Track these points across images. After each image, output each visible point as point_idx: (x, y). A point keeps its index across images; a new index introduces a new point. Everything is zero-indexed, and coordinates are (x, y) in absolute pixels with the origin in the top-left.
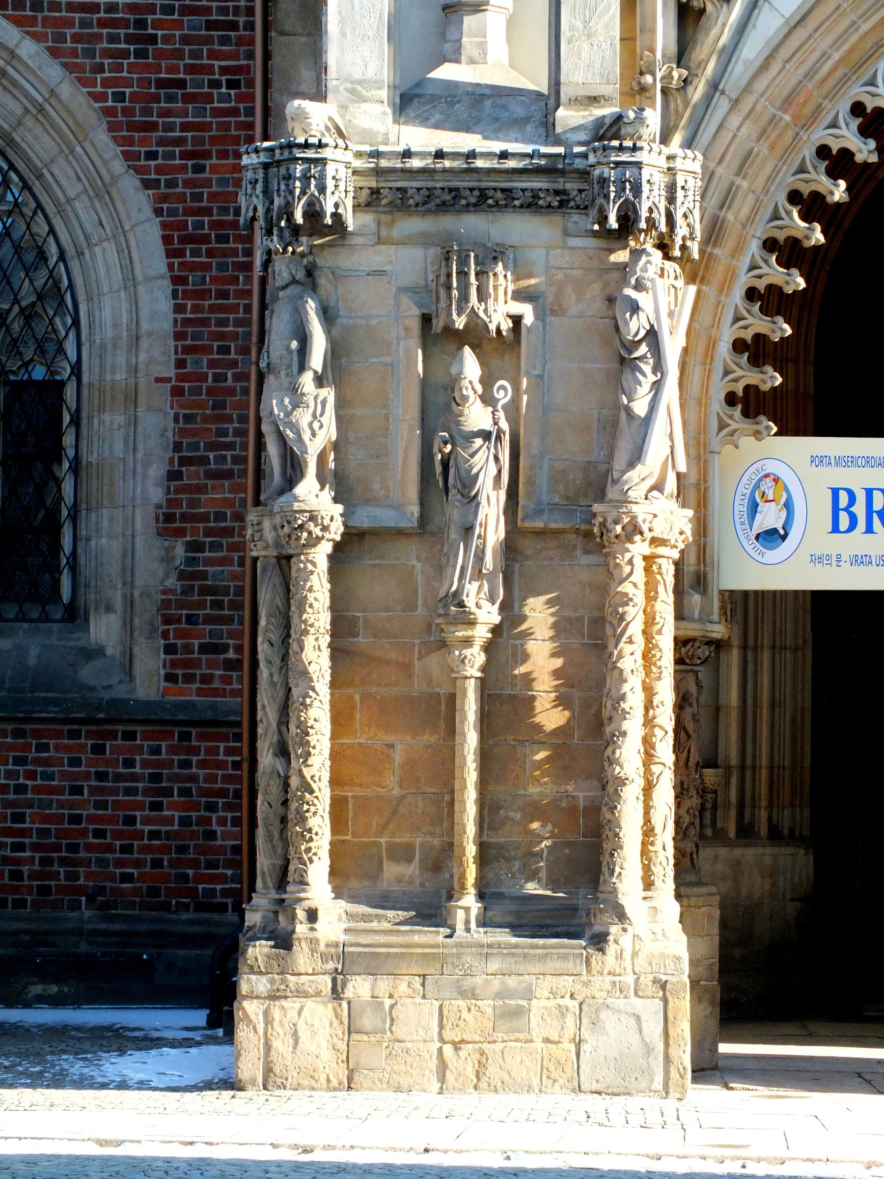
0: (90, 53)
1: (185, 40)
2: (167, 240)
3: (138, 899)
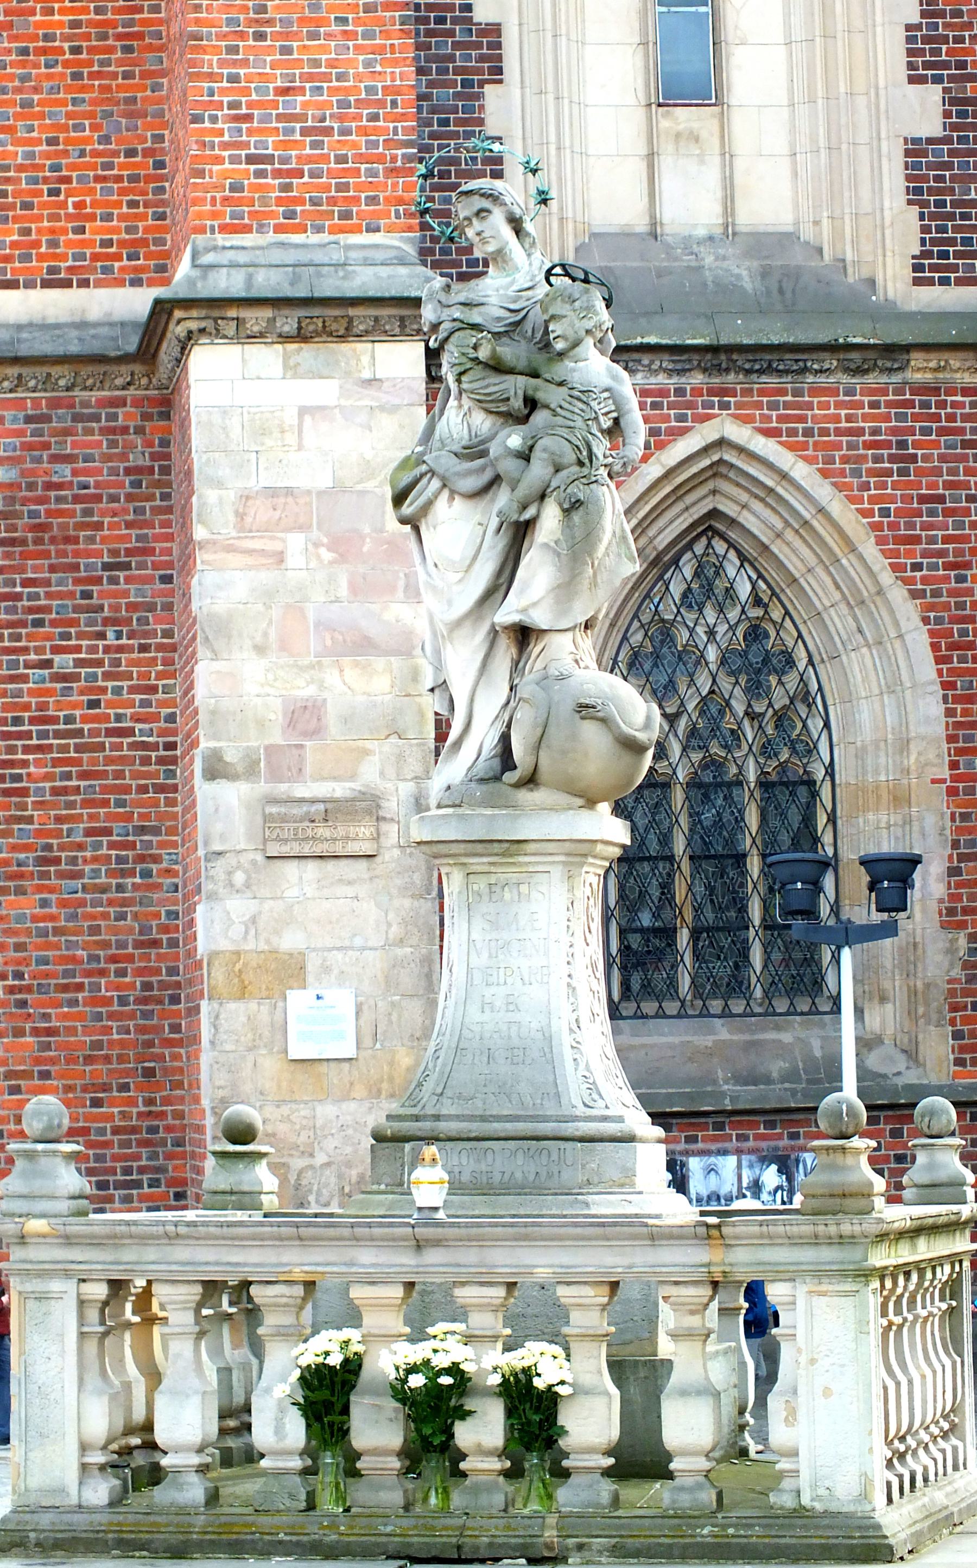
0: (857, 473)
1: (942, 458)
2: (935, 647)
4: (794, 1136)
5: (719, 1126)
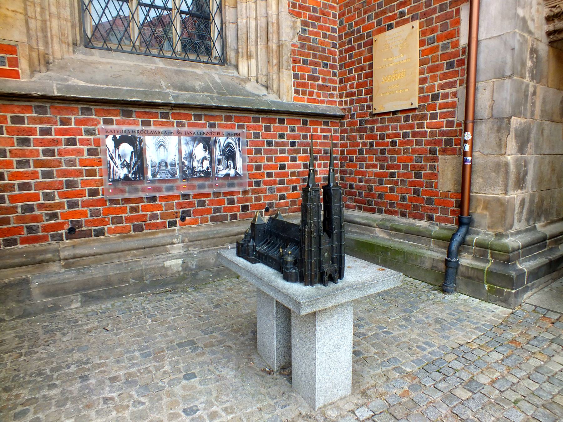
3: (287, 208)
4: (212, 126)
5: (165, 116)
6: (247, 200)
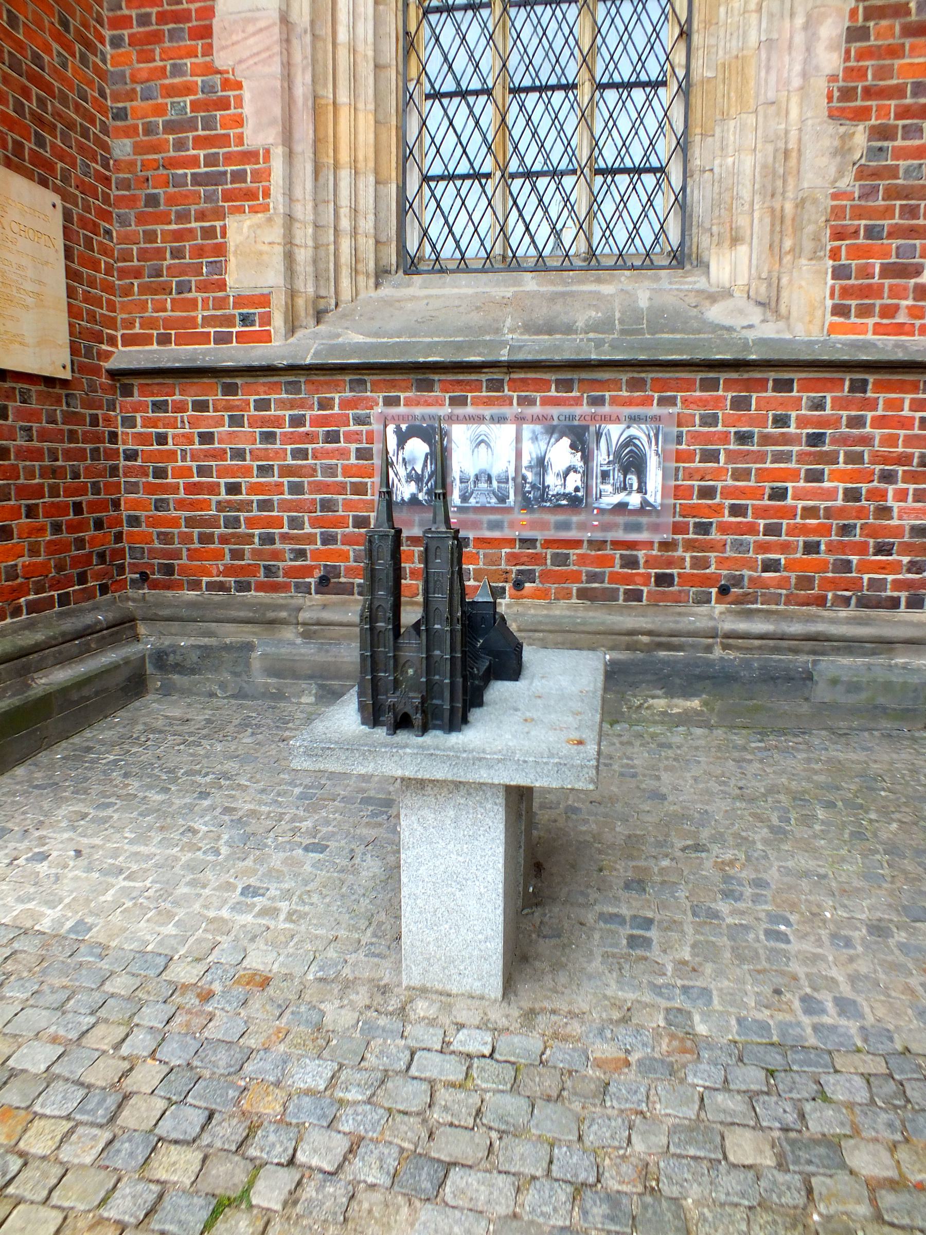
3: (784, 592)
4: (597, 401)
5: (495, 385)
6: (670, 563)
